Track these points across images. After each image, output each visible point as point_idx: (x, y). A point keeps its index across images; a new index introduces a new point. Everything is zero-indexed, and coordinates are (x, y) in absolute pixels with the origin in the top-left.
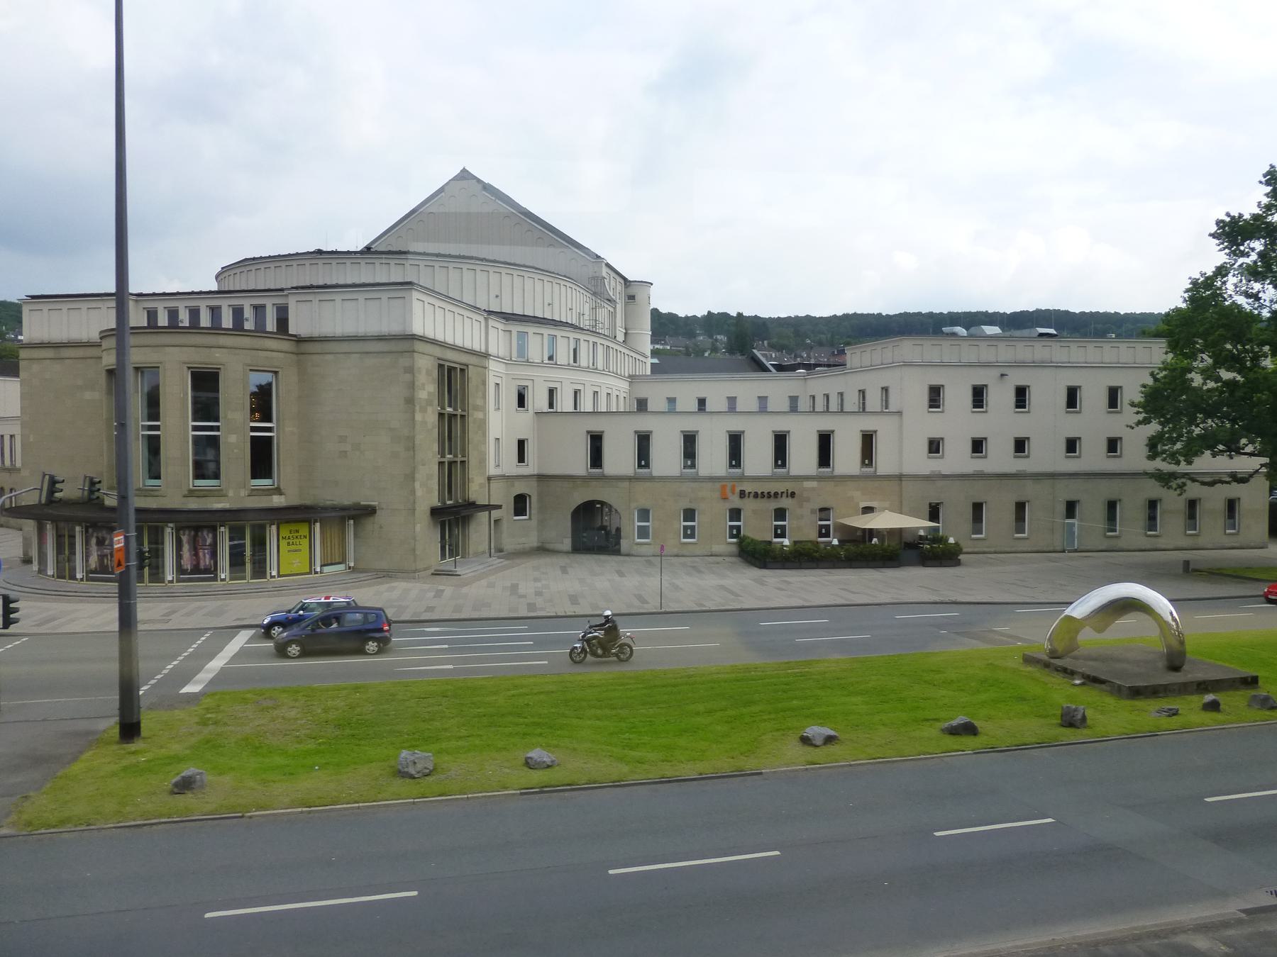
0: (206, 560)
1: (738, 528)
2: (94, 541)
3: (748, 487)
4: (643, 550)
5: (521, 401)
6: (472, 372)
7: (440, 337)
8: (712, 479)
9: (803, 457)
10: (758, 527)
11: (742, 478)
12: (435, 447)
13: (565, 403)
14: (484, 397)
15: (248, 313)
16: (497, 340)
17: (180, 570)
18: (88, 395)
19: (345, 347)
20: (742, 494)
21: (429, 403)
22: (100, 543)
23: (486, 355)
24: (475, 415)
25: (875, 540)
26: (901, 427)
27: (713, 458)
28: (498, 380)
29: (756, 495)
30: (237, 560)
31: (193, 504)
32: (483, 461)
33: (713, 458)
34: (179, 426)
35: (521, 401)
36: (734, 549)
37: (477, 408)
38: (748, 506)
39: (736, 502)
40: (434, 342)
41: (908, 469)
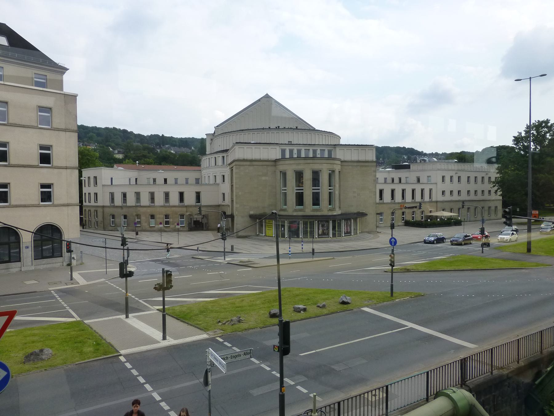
0: (349, 230)
1: (403, 217)
2: (321, 225)
3: (407, 206)
4: (382, 225)
8: (399, 203)
10: (408, 217)
11: (405, 203)
15: (295, 152)
17: (345, 234)
18: (264, 178)
19: (350, 164)
20: (406, 208)
22: (323, 226)
25: (438, 220)
26: (437, 187)
27: (398, 197)
29: (409, 208)
30: (305, 233)
31: (330, 213)
33: (398, 197)
34: (292, 189)
36: (403, 224)
38: (407, 211)
39: (404, 210)
41: (439, 200)
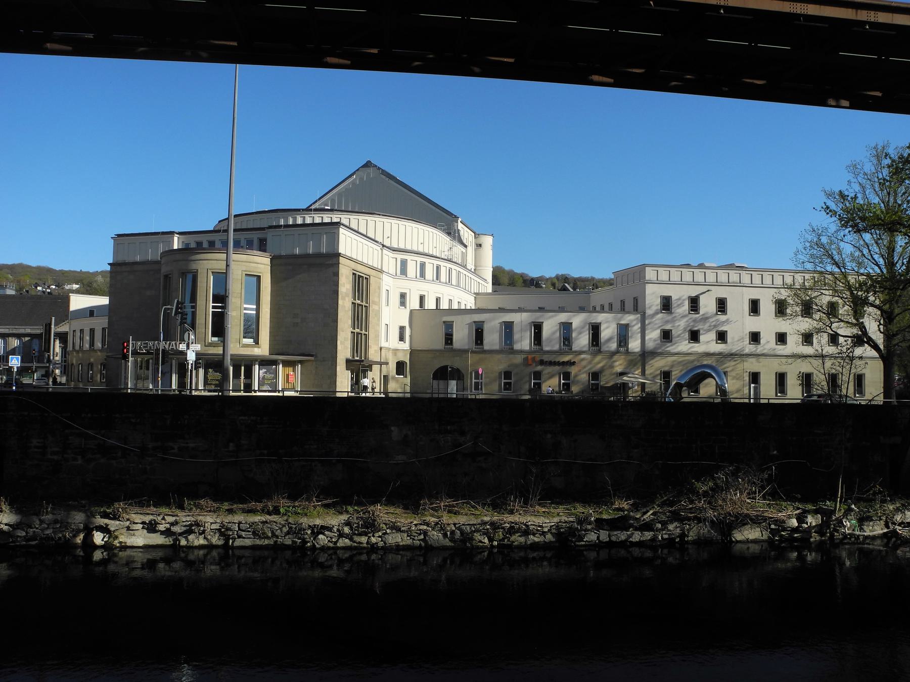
3: (546, 358)
5: (403, 303)
6: (372, 280)
7: (354, 257)
9: (582, 341)
12: (350, 322)
13: (430, 304)
14: (379, 296)
16: (390, 262)
20: (542, 362)
21: (347, 295)
23: (381, 271)
24: (373, 308)
28: (387, 288)
32: (377, 336)
35: (403, 303)
37: (374, 303)
40: (350, 259)
